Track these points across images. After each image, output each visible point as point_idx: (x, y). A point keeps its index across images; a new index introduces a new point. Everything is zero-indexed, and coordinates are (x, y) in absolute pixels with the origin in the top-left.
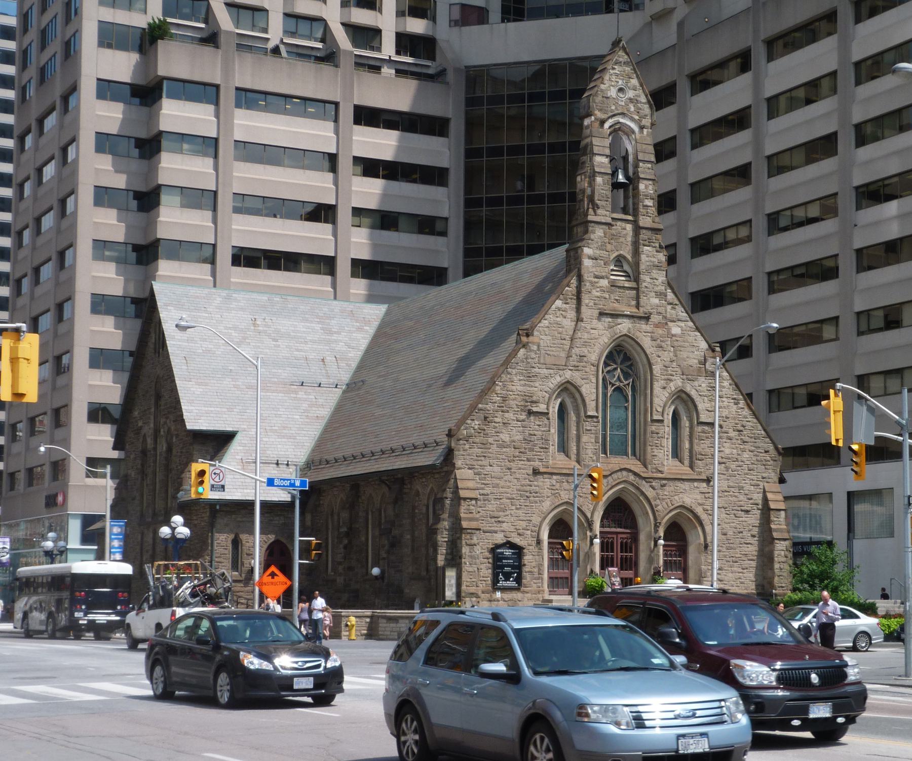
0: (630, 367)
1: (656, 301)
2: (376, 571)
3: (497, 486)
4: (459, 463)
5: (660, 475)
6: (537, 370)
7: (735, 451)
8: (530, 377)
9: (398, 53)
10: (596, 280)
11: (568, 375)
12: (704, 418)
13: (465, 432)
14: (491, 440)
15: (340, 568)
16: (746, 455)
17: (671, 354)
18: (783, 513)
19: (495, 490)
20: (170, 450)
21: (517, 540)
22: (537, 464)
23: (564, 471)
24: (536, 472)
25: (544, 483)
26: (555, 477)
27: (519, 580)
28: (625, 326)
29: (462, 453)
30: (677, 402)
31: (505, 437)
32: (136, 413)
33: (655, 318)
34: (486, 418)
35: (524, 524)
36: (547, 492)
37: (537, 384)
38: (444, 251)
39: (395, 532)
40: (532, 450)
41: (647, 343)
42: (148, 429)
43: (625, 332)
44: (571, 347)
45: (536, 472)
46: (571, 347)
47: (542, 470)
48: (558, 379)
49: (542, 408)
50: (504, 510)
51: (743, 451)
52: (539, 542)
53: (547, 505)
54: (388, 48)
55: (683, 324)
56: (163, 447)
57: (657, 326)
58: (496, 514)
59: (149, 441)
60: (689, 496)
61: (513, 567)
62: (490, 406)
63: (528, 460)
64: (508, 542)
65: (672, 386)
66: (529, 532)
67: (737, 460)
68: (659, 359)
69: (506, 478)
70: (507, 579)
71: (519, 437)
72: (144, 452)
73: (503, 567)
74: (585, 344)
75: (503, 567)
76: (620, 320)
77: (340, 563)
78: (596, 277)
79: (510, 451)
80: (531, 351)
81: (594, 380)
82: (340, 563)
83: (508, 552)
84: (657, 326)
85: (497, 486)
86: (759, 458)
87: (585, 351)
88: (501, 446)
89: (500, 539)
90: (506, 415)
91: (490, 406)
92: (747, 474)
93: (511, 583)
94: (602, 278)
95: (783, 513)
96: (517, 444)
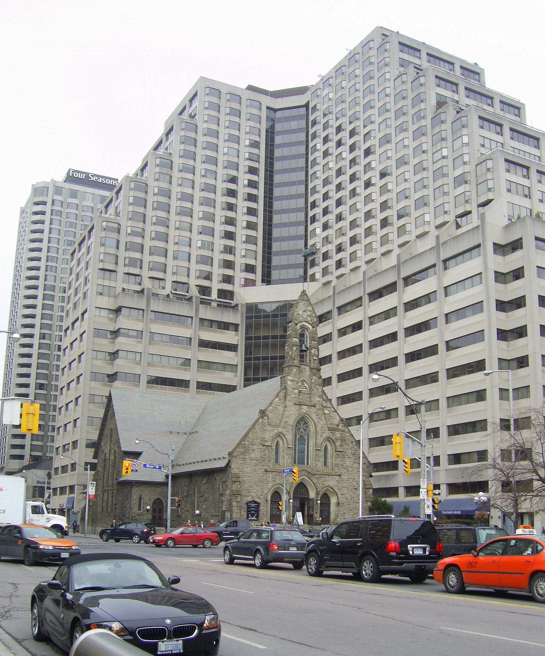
0: (307, 427)
1: (319, 399)
2: (197, 512)
3: (249, 476)
4: (233, 466)
5: (319, 473)
8: (264, 431)
9: (218, 297)
11: (280, 430)
14: (246, 457)
15: (183, 511)
17: (325, 422)
19: (248, 478)
20: (115, 459)
21: (257, 500)
22: (266, 467)
25: (271, 475)
26: (274, 473)
27: (257, 517)
28: (305, 409)
30: (327, 442)
31: (253, 456)
32: (102, 444)
33: (318, 407)
35: (259, 493)
36: (270, 480)
38: (234, 378)
39: (206, 495)
40: (264, 461)
41: (314, 416)
42: (107, 451)
43: (305, 412)
45: (266, 471)
47: (268, 470)
48: (276, 431)
49: (268, 444)
50: (252, 487)
51: (355, 463)
52: (267, 501)
53: (270, 485)
54: (214, 295)
55: (329, 409)
56: (112, 458)
57: (318, 410)
58: (248, 488)
59: (107, 455)
60: (332, 482)
61: (255, 511)
62: (247, 443)
63: (263, 466)
64: (253, 501)
65: (325, 436)
66: (262, 497)
70: (252, 517)
72: (105, 460)
73: (250, 511)
75: (250, 511)
76: (303, 407)
77: (183, 509)
78: (293, 389)
79: (255, 462)
82: (183, 509)
83: (253, 505)
84: (318, 410)
85: (249, 476)
87: (287, 420)
88: (251, 460)
89: (250, 499)
91: (247, 443)
93: (254, 518)
94: (296, 389)
96: (258, 459)
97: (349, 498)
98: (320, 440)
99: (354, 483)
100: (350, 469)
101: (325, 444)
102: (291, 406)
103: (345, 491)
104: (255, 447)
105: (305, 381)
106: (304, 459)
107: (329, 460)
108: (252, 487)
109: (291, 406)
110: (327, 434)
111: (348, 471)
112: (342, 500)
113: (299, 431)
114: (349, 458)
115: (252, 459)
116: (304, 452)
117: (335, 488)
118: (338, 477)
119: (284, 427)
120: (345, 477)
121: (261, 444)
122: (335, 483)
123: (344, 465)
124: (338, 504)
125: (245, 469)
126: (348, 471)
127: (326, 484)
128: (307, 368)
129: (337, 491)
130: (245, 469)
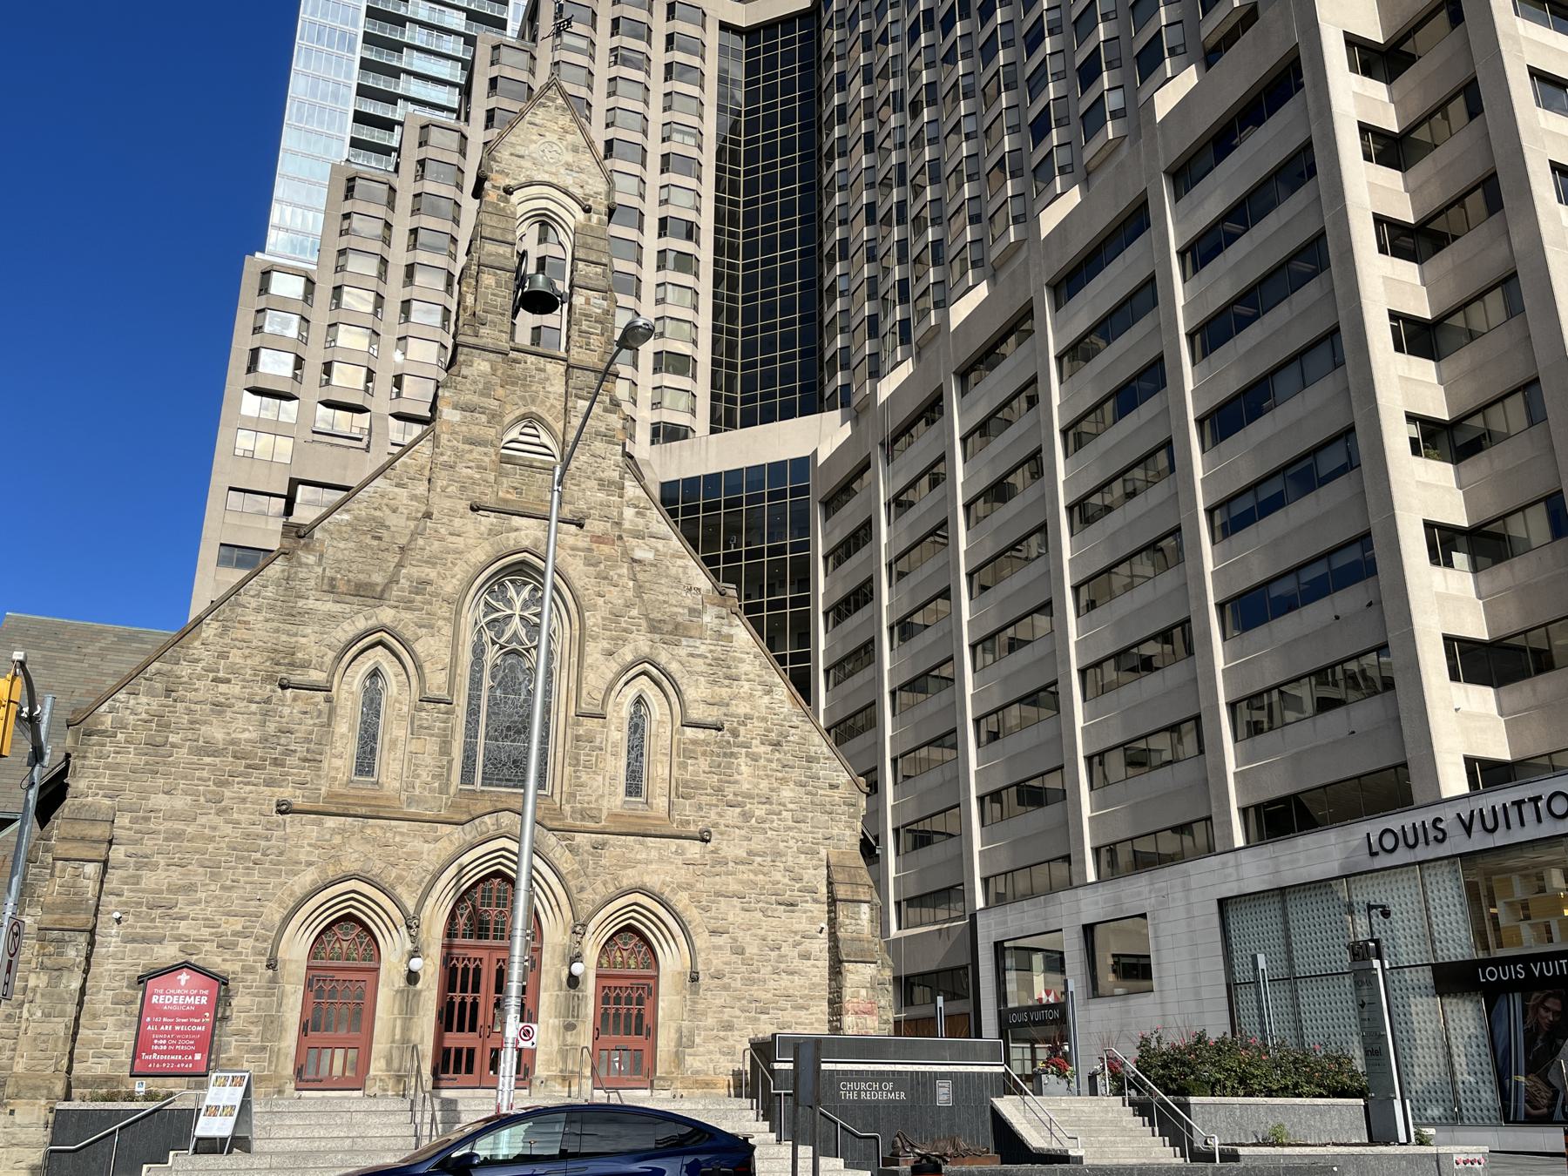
1: (601, 496)
5: (591, 825)
6: (311, 603)
7: (764, 784)
8: (293, 616)
10: (467, 447)
11: (386, 615)
12: (695, 714)
13: (108, 719)
16: (787, 793)
17: (630, 594)
18: (865, 908)
22: (286, 793)
23: (362, 811)
24: (284, 809)
25: (306, 831)
26: (331, 822)
28: (527, 532)
29: (93, 762)
31: (216, 732)
34: (168, 692)
35: (238, 924)
37: (309, 631)
41: (576, 569)
43: (526, 543)
44: (400, 565)
45: (284, 809)
46: (400, 565)
47: (299, 802)
48: (361, 624)
49: (316, 676)
51: (784, 781)
55: (660, 545)
57: (599, 539)
62: (184, 670)
66: (250, 942)
67: (768, 801)
68: (600, 601)
69: (202, 820)
71: (251, 734)
74: (431, 562)
80: (300, 564)
81: (447, 630)
86: (817, 800)
90: (223, 688)
91: (184, 670)
92: (790, 829)
95: (865, 908)
97: (752, 950)
98: (600, 670)
99: (778, 876)
100: (760, 811)
101: (631, 693)
102: (452, 513)
103: (732, 913)
104: (235, 689)
105: (541, 420)
106: (520, 764)
107: (658, 770)
108: (190, 888)
109: (452, 513)
110: (641, 643)
111: (746, 816)
112: (714, 957)
113: (500, 634)
114: (755, 758)
115: (209, 749)
116: (523, 729)
117: (681, 901)
118: (694, 849)
119: (408, 605)
120: (731, 847)
121: (269, 678)
122: (683, 875)
123: (729, 790)
124: (694, 978)
125: (159, 800)
126: (746, 816)
127: (629, 878)
128: (555, 370)
129: (692, 914)
130: (159, 800)
